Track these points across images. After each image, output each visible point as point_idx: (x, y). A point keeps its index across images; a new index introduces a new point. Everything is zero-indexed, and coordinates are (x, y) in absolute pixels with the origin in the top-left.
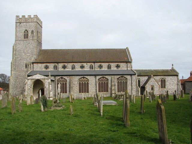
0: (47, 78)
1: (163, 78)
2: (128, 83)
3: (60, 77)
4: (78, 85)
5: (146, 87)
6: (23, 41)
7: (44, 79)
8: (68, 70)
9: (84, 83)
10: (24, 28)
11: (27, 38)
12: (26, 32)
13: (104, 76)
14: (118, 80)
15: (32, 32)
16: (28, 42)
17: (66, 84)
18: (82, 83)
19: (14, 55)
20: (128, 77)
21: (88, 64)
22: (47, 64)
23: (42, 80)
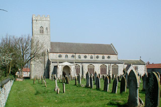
6: (39, 35)
16: (44, 36)
18: (90, 69)
22: (61, 54)
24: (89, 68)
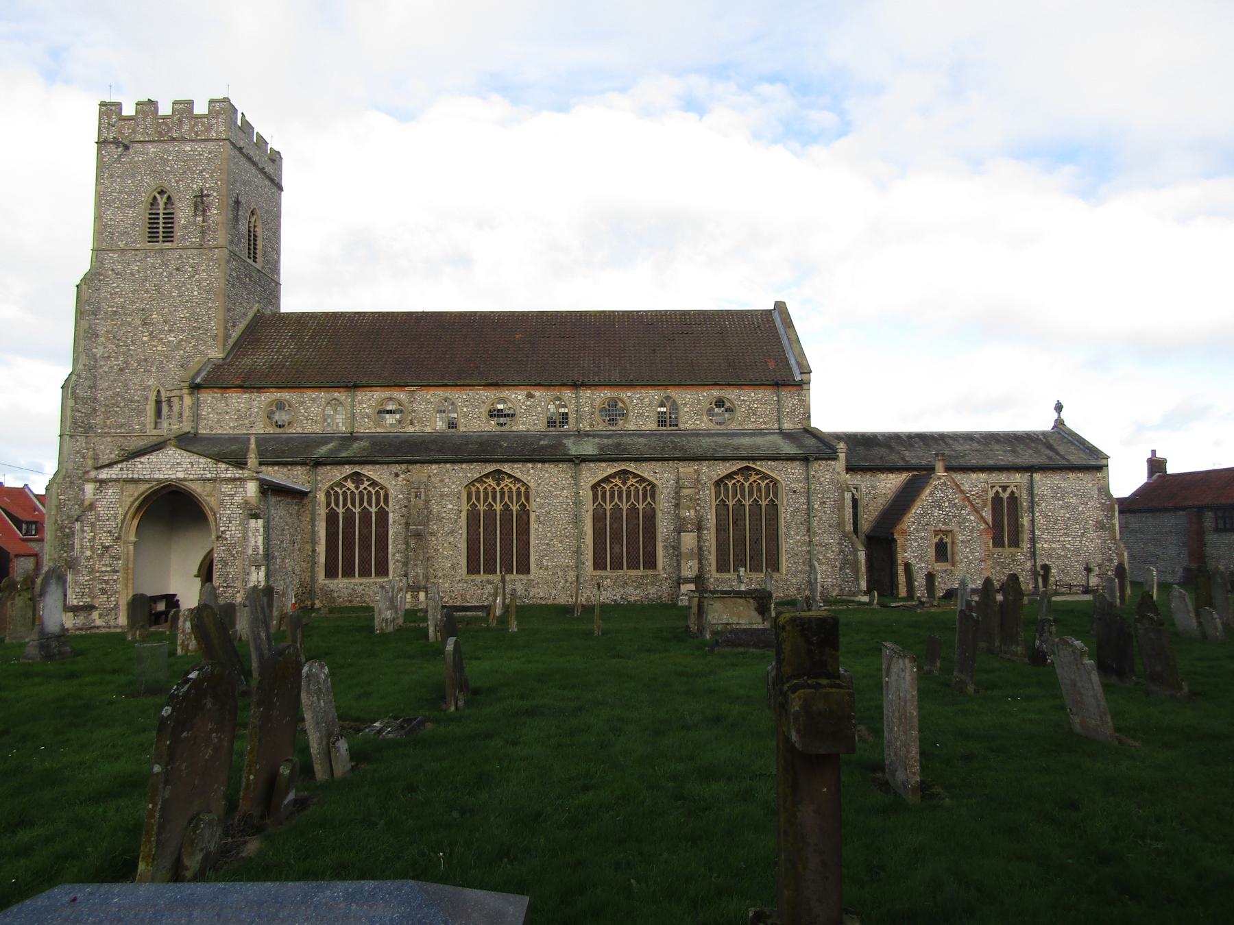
0: (232, 473)
1: (1004, 488)
2: (785, 514)
3: (348, 470)
4: (463, 522)
5: (903, 532)
7: (214, 480)
8: (411, 429)
9: (498, 507)
10: (147, 179)
11: (169, 236)
12: (161, 201)
13: (631, 467)
14: (718, 495)
15: (200, 203)
17: (383, 516)
18: (491, 513)
19: (85, 335)
20: (789, 475)
21: (537, 394)
23: (197, 488)
24: (482, 507)
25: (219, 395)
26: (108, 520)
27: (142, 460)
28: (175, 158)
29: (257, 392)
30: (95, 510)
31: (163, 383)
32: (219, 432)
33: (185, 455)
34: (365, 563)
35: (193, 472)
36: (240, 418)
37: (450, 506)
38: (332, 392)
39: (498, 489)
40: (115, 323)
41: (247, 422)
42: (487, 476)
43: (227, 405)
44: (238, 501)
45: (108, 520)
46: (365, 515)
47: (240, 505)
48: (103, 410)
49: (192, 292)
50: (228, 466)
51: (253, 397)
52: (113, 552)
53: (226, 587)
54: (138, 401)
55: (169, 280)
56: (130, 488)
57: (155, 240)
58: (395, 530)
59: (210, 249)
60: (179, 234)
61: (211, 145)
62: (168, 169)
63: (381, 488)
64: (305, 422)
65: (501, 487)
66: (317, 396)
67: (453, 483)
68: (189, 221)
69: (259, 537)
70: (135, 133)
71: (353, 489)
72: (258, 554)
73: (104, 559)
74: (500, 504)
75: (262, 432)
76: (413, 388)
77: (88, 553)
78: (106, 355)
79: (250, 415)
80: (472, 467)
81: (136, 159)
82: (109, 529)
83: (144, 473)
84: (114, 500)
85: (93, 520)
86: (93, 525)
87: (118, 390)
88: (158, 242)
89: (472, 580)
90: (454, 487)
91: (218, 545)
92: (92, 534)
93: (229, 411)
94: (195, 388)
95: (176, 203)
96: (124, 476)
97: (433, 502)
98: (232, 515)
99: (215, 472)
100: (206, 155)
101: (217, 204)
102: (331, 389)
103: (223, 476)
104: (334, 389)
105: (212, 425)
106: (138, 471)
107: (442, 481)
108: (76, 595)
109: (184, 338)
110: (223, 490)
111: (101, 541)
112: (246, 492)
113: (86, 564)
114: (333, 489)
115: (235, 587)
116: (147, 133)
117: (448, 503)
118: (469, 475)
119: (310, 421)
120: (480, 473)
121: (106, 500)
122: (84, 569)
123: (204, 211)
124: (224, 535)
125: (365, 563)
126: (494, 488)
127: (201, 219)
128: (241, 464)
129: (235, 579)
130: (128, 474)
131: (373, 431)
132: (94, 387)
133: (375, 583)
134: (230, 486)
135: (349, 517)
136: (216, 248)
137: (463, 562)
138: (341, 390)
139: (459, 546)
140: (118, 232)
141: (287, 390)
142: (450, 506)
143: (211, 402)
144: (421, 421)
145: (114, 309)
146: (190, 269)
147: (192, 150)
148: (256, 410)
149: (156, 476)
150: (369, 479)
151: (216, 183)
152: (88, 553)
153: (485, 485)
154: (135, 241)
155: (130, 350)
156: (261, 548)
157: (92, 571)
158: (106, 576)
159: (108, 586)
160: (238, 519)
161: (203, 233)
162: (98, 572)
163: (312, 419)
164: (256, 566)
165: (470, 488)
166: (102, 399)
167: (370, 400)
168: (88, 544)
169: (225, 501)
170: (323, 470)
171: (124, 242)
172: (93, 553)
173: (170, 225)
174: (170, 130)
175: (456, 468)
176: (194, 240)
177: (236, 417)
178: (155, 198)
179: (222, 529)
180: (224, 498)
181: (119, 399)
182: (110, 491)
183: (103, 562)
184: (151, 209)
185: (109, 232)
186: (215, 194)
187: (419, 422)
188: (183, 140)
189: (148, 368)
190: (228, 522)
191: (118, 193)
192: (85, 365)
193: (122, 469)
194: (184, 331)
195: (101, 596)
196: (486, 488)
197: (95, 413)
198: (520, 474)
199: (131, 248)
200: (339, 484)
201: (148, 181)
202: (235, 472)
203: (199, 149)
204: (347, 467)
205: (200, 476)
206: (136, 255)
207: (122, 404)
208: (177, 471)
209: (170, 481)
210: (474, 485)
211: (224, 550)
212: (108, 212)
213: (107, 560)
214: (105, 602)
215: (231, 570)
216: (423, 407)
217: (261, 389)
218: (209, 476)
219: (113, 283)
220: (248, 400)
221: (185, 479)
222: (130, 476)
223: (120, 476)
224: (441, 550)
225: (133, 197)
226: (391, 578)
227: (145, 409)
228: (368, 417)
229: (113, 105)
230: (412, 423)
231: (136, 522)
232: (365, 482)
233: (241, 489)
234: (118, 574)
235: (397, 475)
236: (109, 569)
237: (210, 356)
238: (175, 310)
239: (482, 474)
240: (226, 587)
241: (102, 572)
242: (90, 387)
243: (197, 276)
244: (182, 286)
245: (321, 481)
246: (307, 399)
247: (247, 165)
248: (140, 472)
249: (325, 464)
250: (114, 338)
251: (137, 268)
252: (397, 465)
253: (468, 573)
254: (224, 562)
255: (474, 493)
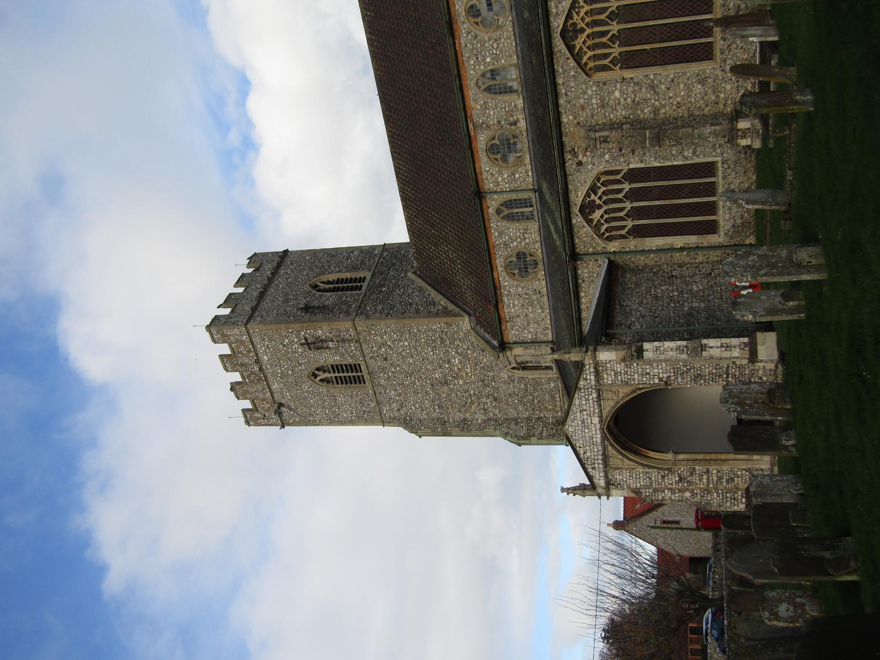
0: (589, 375)
3: (578, 220)
7: (599, 392)
8: (522, 124)
9: (615, 28)
11: (355, 368)
12: (323, 376)
15: (315, 345)
17: (633, 175)
18: (624, 38)
19: (465, 428)
23: (609, 406)
24: (616, 50)
25: (508, 324)
26: (650, 479)
27: (582, 452)
28: (278, 368)
29: (500, 290)
30: (639, 489)
31: (504, 366)
32: (549, 322)
33: (572, 417)
34: (695, 191)
35: (592, 409)
36: (531, 304)
37: (617, 94)
38: (488, 216)
39: (588, 31)
40: (450, 406)
41: (534, 297)
42: (571, 48)
43: (518, 316)
44: (622, 368)
45: (650, 479)
46: (633, 195)
47: (626, 366)
48: (538, 412)
49: (406, 346)
50: (582, 379)
51: (506, 293)
52: (686, 474)
53: (728, 374)
54: (526, 385)
55: (398, 366)
56: (612, 462)
57: (361, 378)
58: (653, 159)
59: (358, 334)
60: (350, 361)
61: (256, 340)
62: (290, 372)
63: (599, 179)
64: (527, 241)
65: (585, 27)
66: (496, 230)
67: (585, 93)
68: (336, 353)
69: (665, 347)
70: (266, 399)
71: (601, 211)
72: (686, 347)
73: (694, 481)
74: (609, 24)
75: (544, 282)
76: (471, 127)
77: (687, 494)
78: (483, 412)
79: (526, 294)
80: (561, 70)
81: (289, 397)
82: (660, 477)
83: (596, 450)
84: (628, 474)
85: (651, 491)
86: (656, 490)
87: (516, 401)
88: (363, 376)
89: (722, 53)
90: (589, 92)
91: (676, 384)
92: (666, 491)
93: (524, 315)
94: (503, 346)
95: (322, 364)
96: (601, 466)
97: (612, 116)
98: (640, 373)
99: (590, 390)
100: (267, 343)
101: (312, 331)
102: (486, 217)
103: (593, 382)
104: (485, 214)
105: (541, 328)
106: (594, 456)
107: (583, 108)
108: (734, 505)
109: (454, 350)
110: (610, 382)
111: (674, 484)
112: (610, 361)
113: (699, 496)
114: (604, 234)
115: (728, 367)
116: (262, 390)
117: (613, 97)
118: (572, 74)
119: (526, 236)
120: (568, 59)
121: (628, 481)
122: (705, 498)
123: (322, 341)
124: (664, 379)
125: (695, 191)
126: (588, 36)
127: (330, 343)
128: (579, 366)
129: (718, 367)
130: (599, 464)
131: (529, 167)
132: (516, 419)
133: (725, 177)
134: (605, 376)
135: (636, 213)
136: (356, 329)
137: (694, 68)
138: (484, 206)
139: (672, 76)
140: (362, 408)
141: (493, 262)
142: (617, 94)
143: (517, 330)
144: (510, 113)
145: (437, 407)
146: (383, 349)
147: (266, 355)
148: (520, 289)
149: (599, 441)
150: (588, 195)
151: (291, 333)
152: (687, 494)
153: (585, 49)
154: (367, 395)
155: (474, 394)
156: (679, 343)
157: (708, 491)
158: (712, 479)
159: (725, 477)
160: (644, 367)
161: (344, 341)
162: (708, 485)
163: (524, 234)
164: (702, 350)
165: (590, 69)
166: (527, 413)
167: (492, 174)
168: (677, 495)
169: (623, 380)
170: (580, 248)
171: (370, 403)
172: (687, 490)
173: (344, 368)
174: (252, 373)
175: (563, 91)
176: (353, 348)
177: (530, 308)
178: (322, 380)
179: (657, 381)
180: (620, 381)
181: (525, 400)
182: (618, 477)
183: (698, 481)
184: (333, 383)
185: (364, 414)
186: (303, 333)
187: (512, 115)
188: (258, 361)
189: (490, 378)
190: (648, 376)
191: (325, 409)
192: (495, 429)
193: (593, 468)
194: (447, 351)
195: (736, 482)
196: (588, 48)
197: (542, 418)
198: (564, 3)
199: (374, 397)
200: (597, 228)
201: (306, 387)
202: (588, 372)
203: (263, 349)
204: (574, 221)
205: (595, 403)
206: (380, 393)
207: (530, 397)
208: (592, 423)
209: (603, 430)
210: (586, 64)
211: (683, 379)
212: (345, 416)
213: (695, 478)
214: (742, 479)
215: (707, 371)
216: (492, 113)
217: (496, 288)
218: (595, 395)
219: (411, 409)
220: (510, 297)
221: (600, 417)
222: (600, 462)
223: (601, 470)
224: (679, 100)
225: (325, 398)
226: (719, 159)
227: (533, 379)
228: (513, 174)
229: (246, 416)
230: (515, 123)
231: (652, 454)
232: (592, 198)
233: (608, 365)
234: (710, 470)
235: (580, 164)
236: (705, 477)
237: (469, 328)
238: (428, 360)
239: (569, 55)
240: (728, 374)
241: (708, 482)
242: (517, 424)
243: (389, 343)
244: (402, 356)
245: (594, 248)
246: (501, 241)
247: (268, 298)
248: (596, 454)
249: (573, 245)
250: (464, 406)
251: (393, 392)
252: (567, 164)
253: (711, 59)
254: (698, 378)
255: (597, 63)
